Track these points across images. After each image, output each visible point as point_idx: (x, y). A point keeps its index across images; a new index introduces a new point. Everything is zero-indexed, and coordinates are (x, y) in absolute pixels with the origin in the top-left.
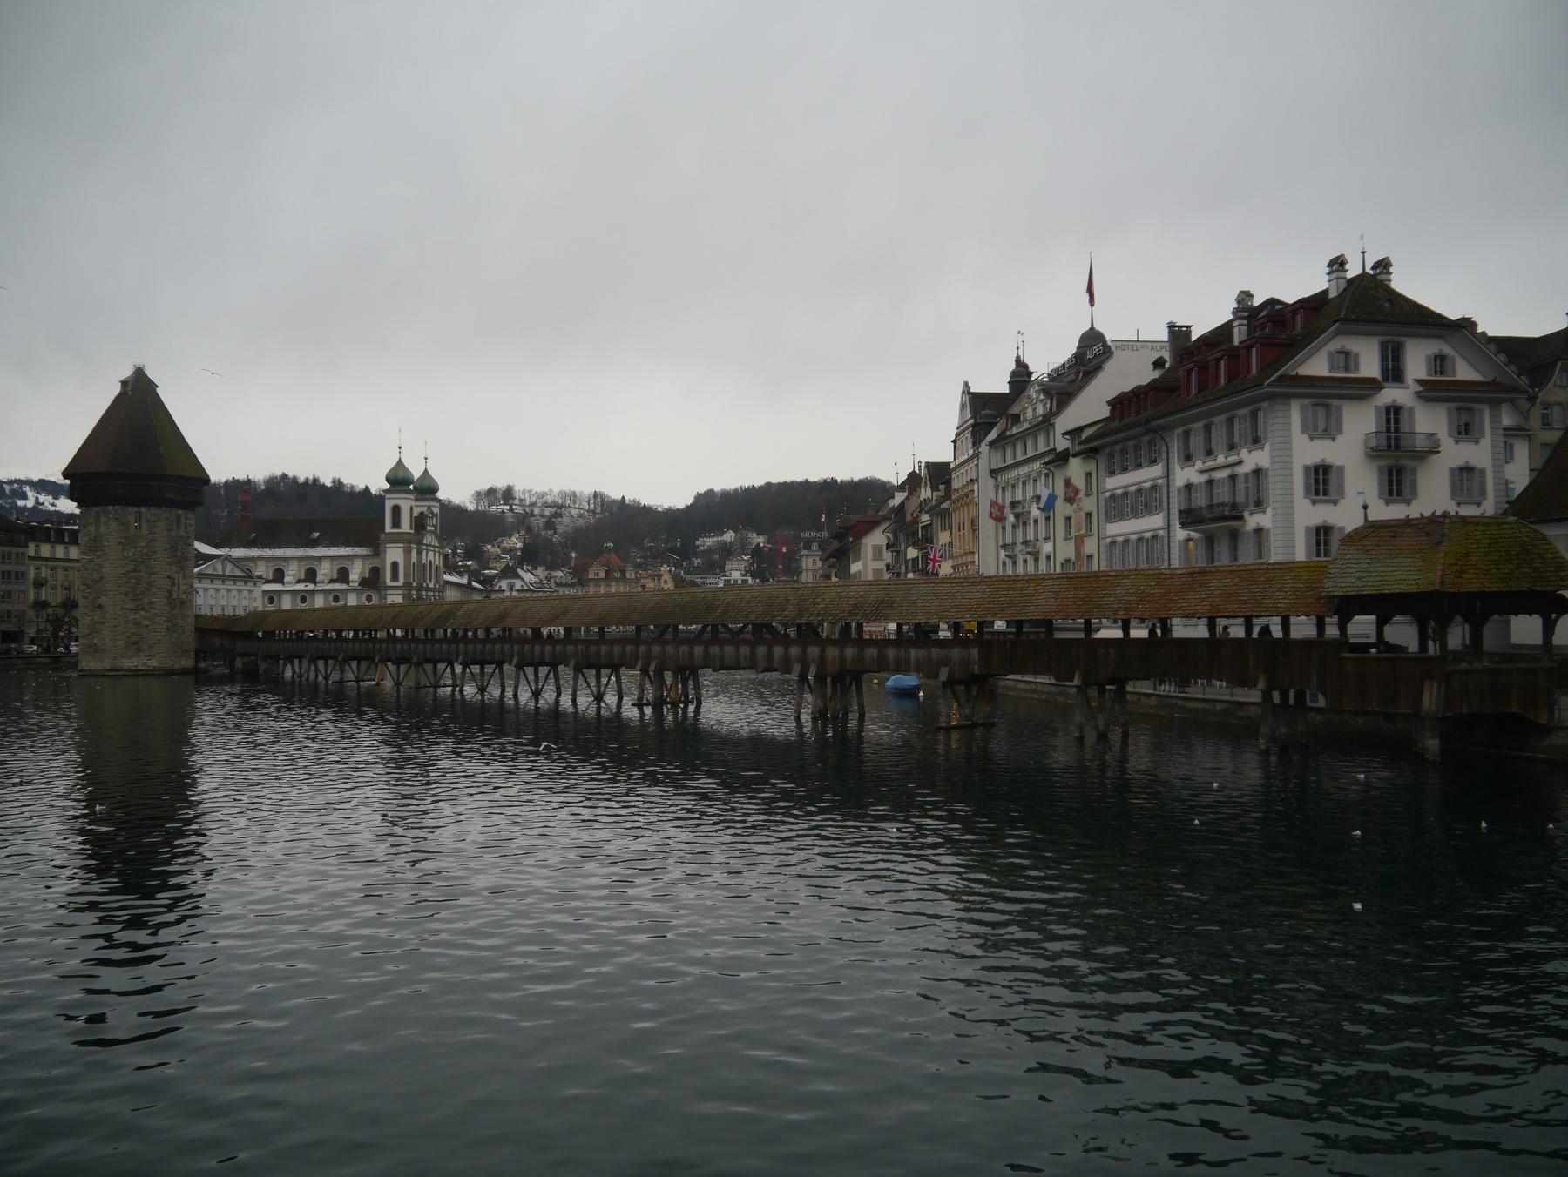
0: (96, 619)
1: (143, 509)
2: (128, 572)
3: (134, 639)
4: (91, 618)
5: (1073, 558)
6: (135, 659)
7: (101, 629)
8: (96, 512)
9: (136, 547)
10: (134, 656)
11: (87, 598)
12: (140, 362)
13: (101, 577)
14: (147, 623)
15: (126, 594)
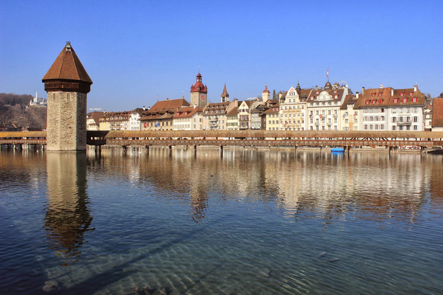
0: (68, 132)
1: (83, 94)
2: (79, 116)
3: (81, 139)
4: (66, 132)
5: (349, 127)
6: (81, 146)
7: (71, 136)
8: (68, 94)
9: (81, 107)
10: (80, 145)
11: (64, 124)
12: (69, 40)
13: (71, 117)
14: (83, 134)
15: (79, 123)
